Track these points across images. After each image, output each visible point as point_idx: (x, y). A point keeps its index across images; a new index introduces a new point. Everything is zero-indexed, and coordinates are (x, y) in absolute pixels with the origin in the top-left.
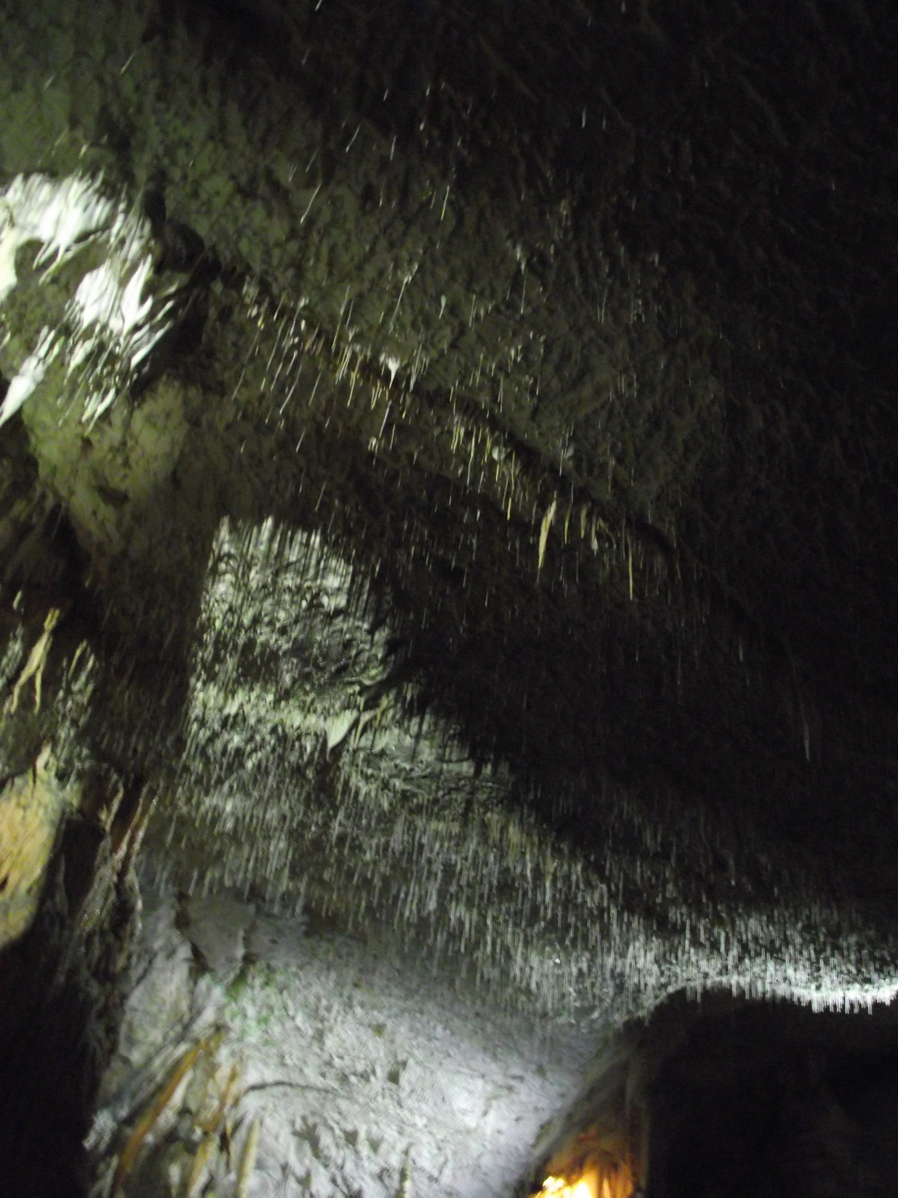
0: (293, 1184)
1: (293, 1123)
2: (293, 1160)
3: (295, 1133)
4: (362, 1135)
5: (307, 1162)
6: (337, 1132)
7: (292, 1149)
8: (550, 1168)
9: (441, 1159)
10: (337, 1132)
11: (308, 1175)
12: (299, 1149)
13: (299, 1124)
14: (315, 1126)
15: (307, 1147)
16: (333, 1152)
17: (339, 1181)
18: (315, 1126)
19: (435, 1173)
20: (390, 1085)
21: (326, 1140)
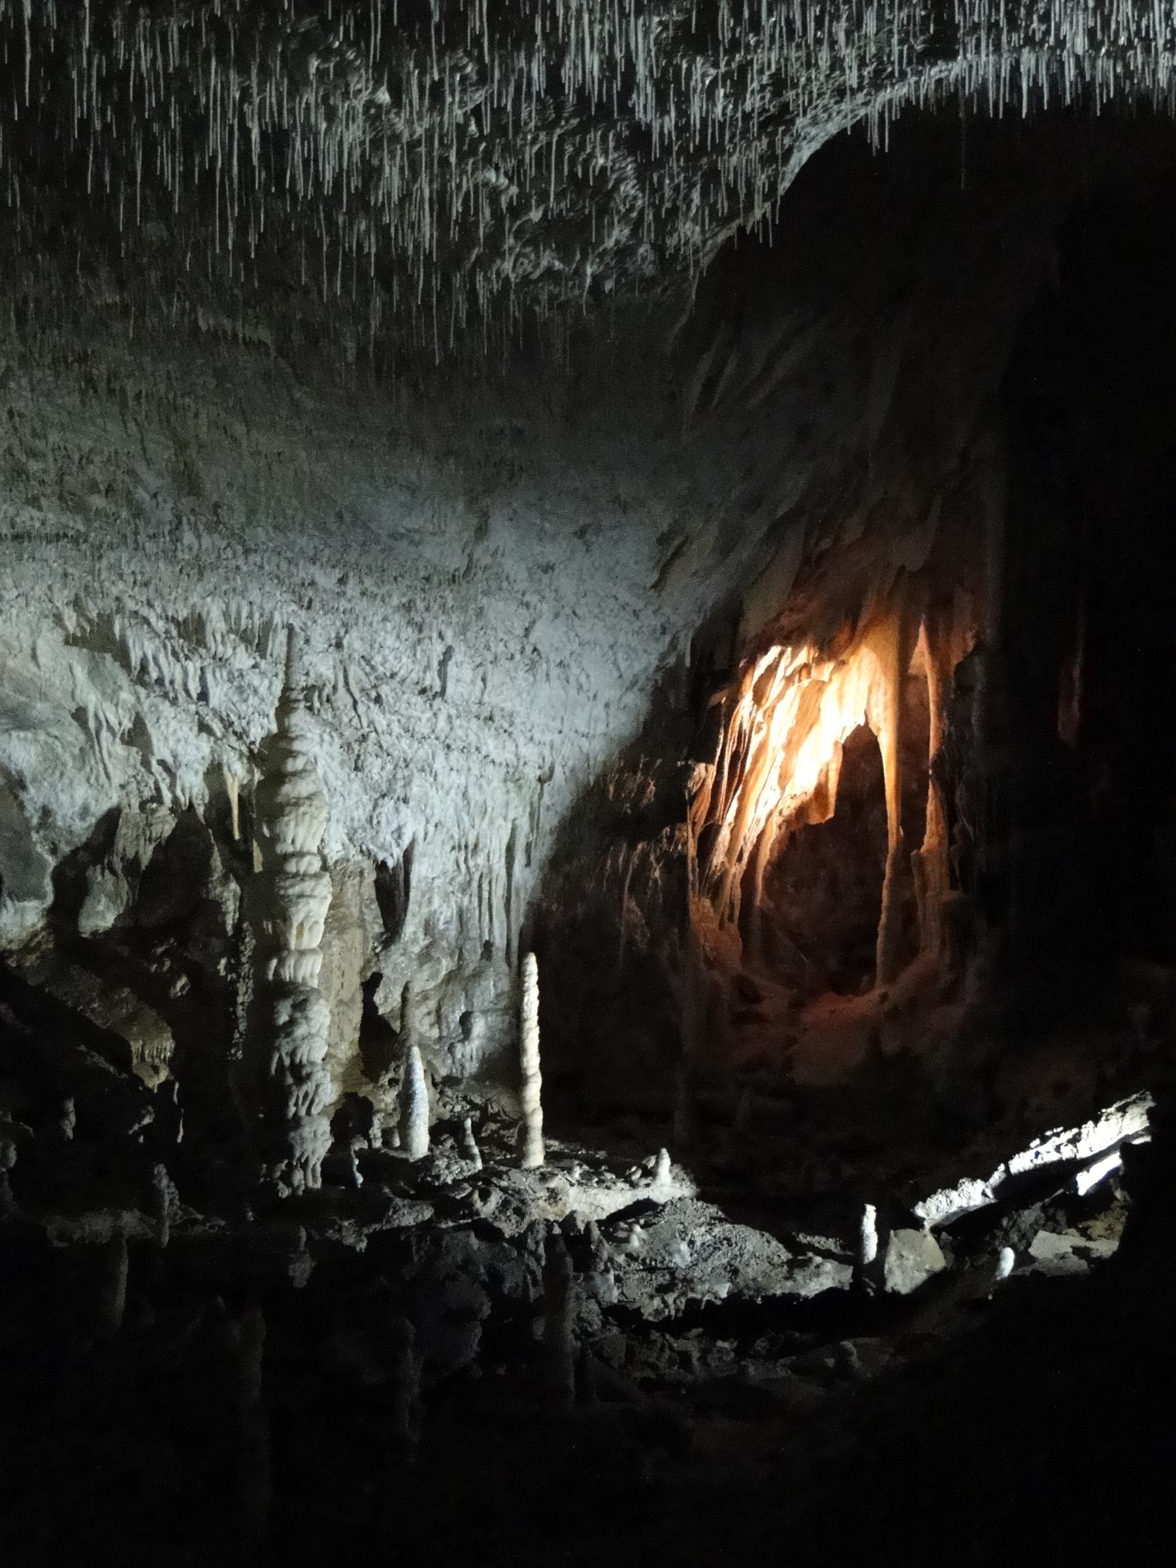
0: (113, 749)
1: (58, 619)
2: (91, 699)
3: (71, 641)
4: (216, 623)
5: (125, 696)
6: (160, 626)
7: (80, 673)
8: (752, 625)
9: (439, 648)
10: (160, 626)
11: (139, 722)
12: (94, 672)
13: (71, 620)
14: (106, 621)
15: (110, 664)
16: (170, 669)
17: (217, 727)
18: (106, 621)
19: (432, 679)
20: (186, 502)
21: (141, 646)
